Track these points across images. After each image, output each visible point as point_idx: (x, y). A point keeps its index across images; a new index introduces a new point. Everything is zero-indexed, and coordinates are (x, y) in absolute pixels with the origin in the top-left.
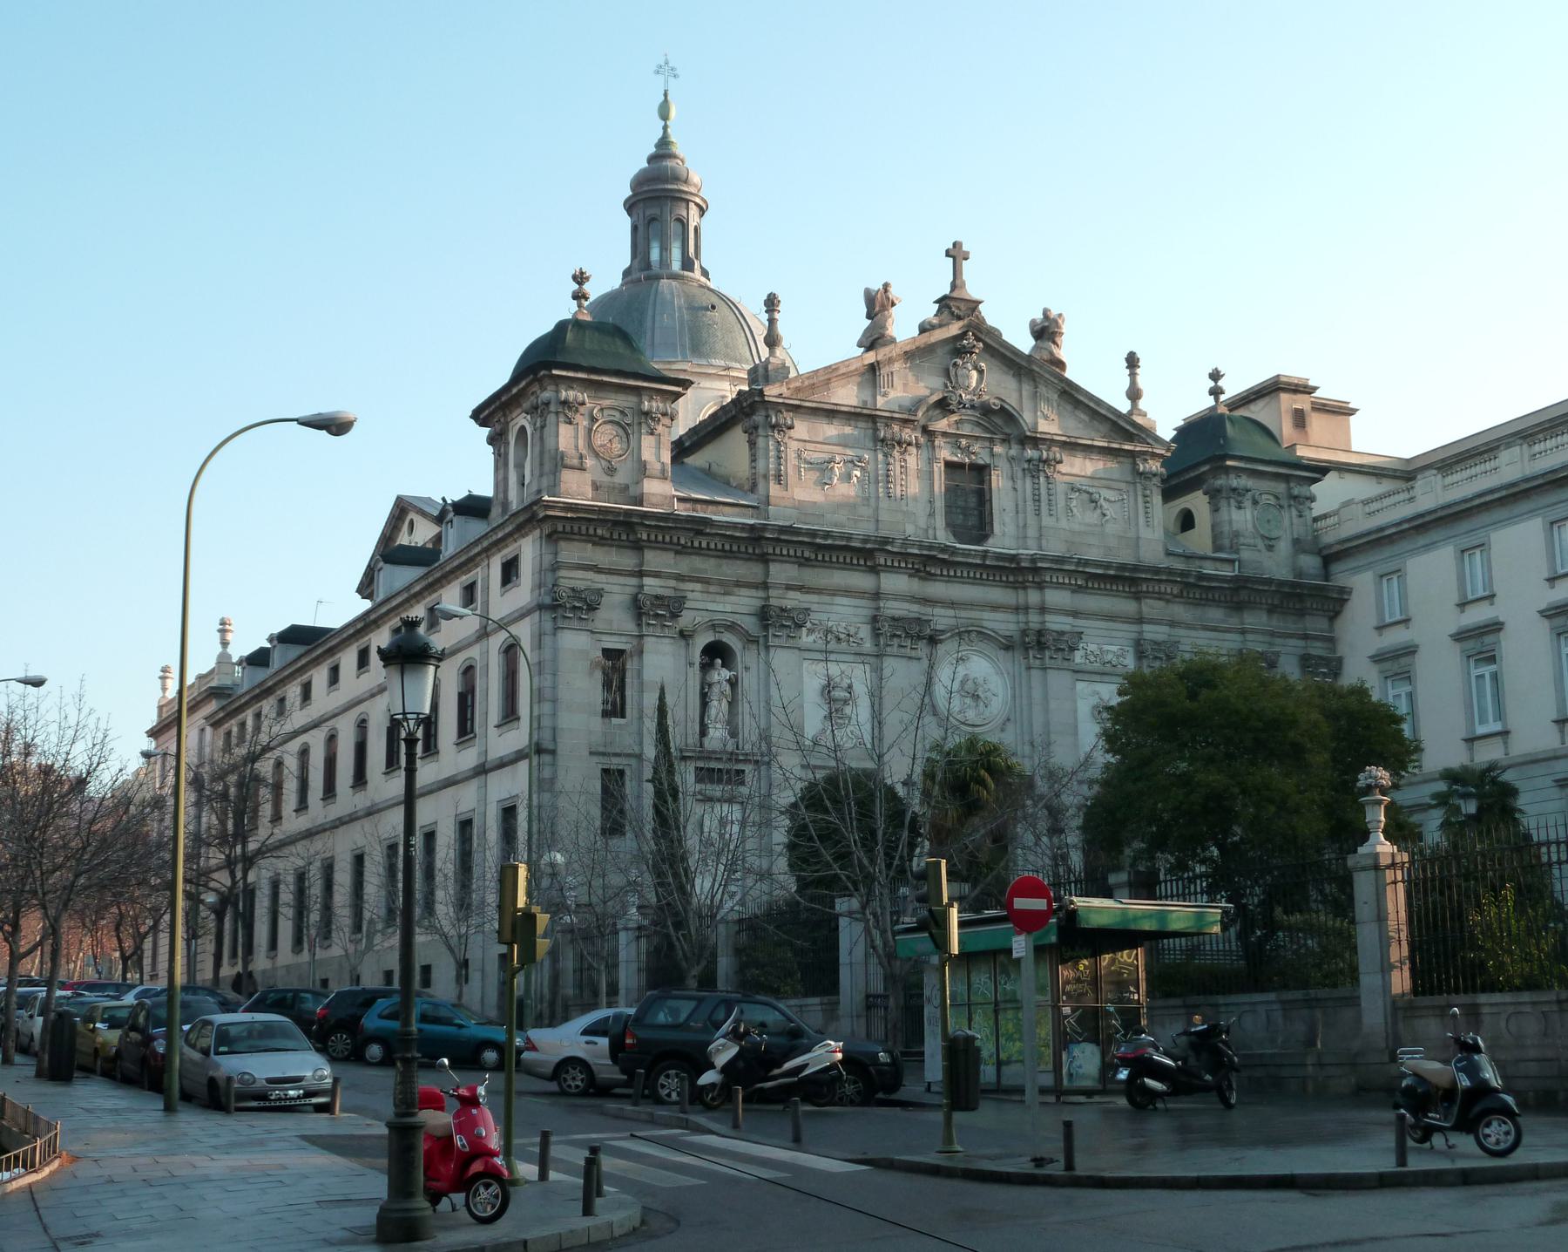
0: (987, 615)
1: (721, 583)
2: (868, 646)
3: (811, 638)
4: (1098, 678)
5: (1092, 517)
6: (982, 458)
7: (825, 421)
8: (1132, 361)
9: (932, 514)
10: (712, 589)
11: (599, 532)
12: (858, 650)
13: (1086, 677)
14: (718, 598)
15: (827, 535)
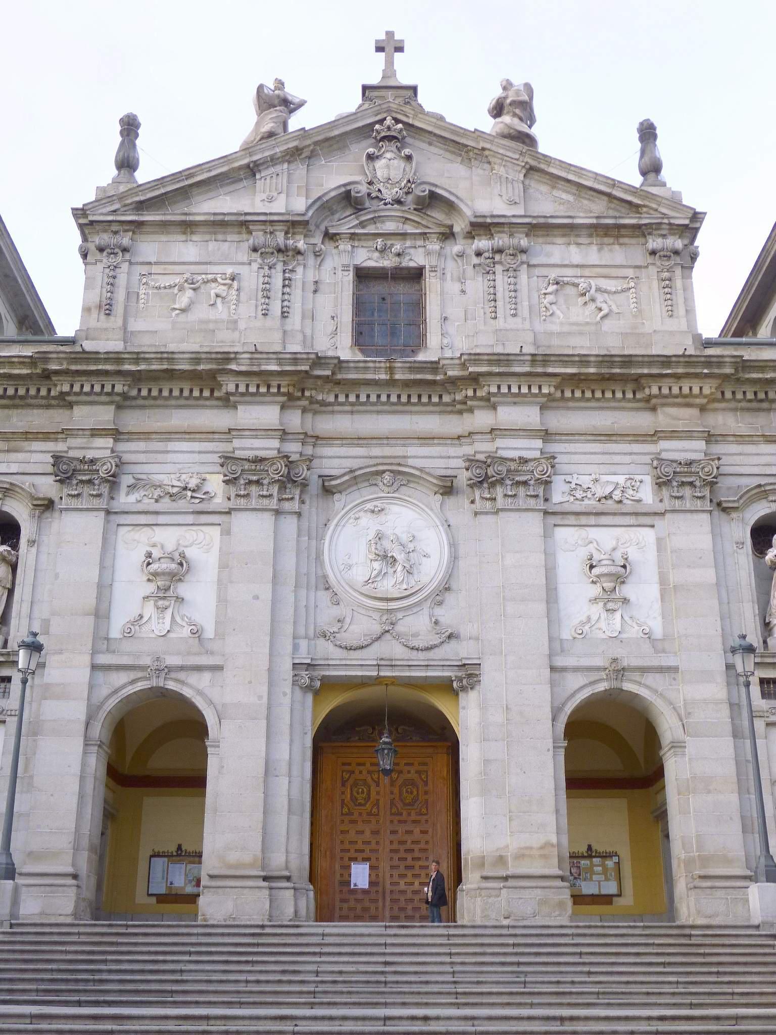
0: (412, 451)
3: (132, 498)
4: (592, 520)
5: (580, 313)
6: (417, 258)
7: (183, 238)
8: (648, 133)
9: (335, 333)
13: (572, 520)
15: (137, 358)
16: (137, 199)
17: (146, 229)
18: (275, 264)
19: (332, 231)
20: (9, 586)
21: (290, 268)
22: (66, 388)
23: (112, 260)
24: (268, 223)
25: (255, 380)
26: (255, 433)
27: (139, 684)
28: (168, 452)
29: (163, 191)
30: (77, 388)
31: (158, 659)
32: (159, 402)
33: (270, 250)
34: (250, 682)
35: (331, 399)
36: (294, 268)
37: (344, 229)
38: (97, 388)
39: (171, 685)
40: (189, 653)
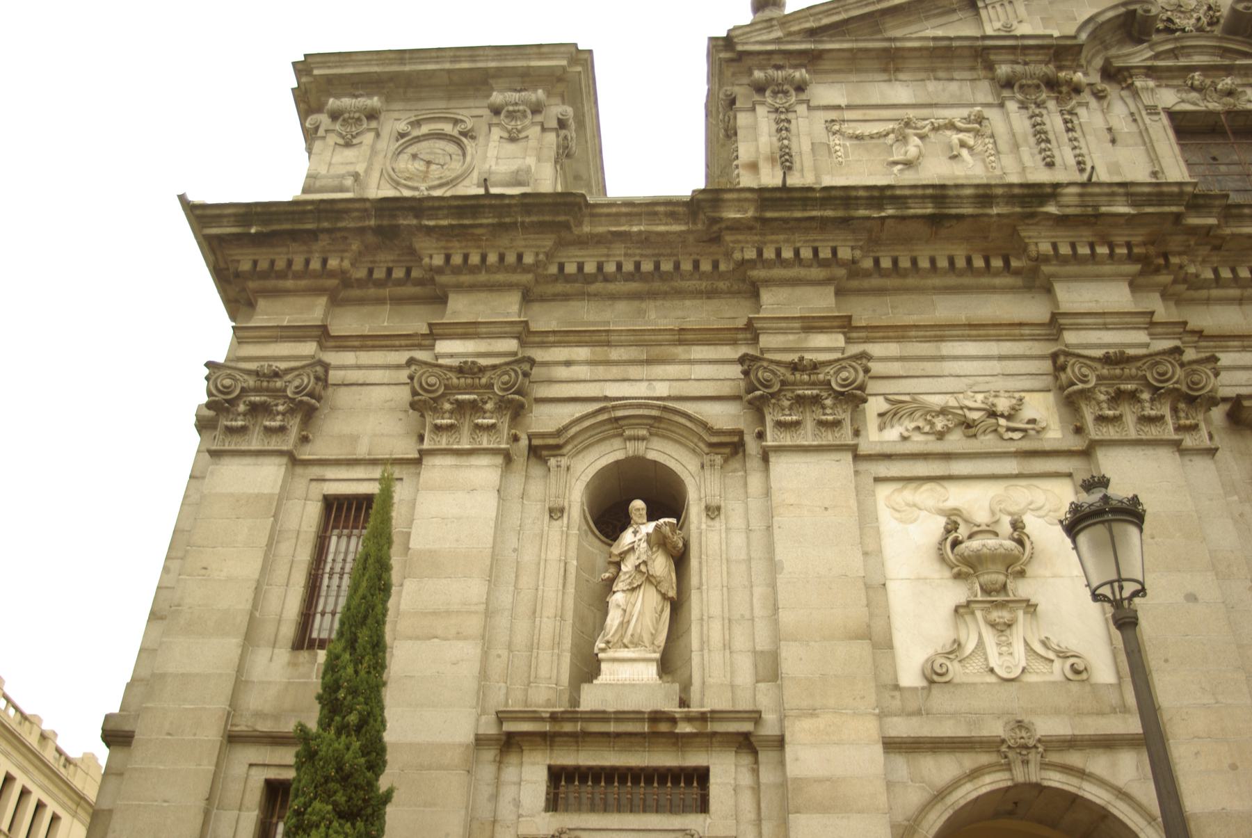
1: (638, 338)
2: (1056, 434)
3: (892, 433)
10: (615, 354)
11: (333, 263)
12: (1026, 445)
14: (634, 371)
16: (808, 25)
17: (826, 65)
18: (1044, 102)
19: (1118, 63)
20: (672, 593)
21: (1068, 108)
22: (751, 254)
23: (780, 101)
24: (1020, 49)
25: (1086, 234)
26: (1100, 321)
27: (988, 779)
28: (943, 358)
29: (844, 16)
30: (769, 253)
31: (1020, 724)
32: (910, 281)
33: (1036, 81)
34: (1234, 767)
35: (1209, 274)
36: (1073, 108)
37: (1135, 61)
38: (806, 253)
39: (1055, 780)
40: (1080, 713)
